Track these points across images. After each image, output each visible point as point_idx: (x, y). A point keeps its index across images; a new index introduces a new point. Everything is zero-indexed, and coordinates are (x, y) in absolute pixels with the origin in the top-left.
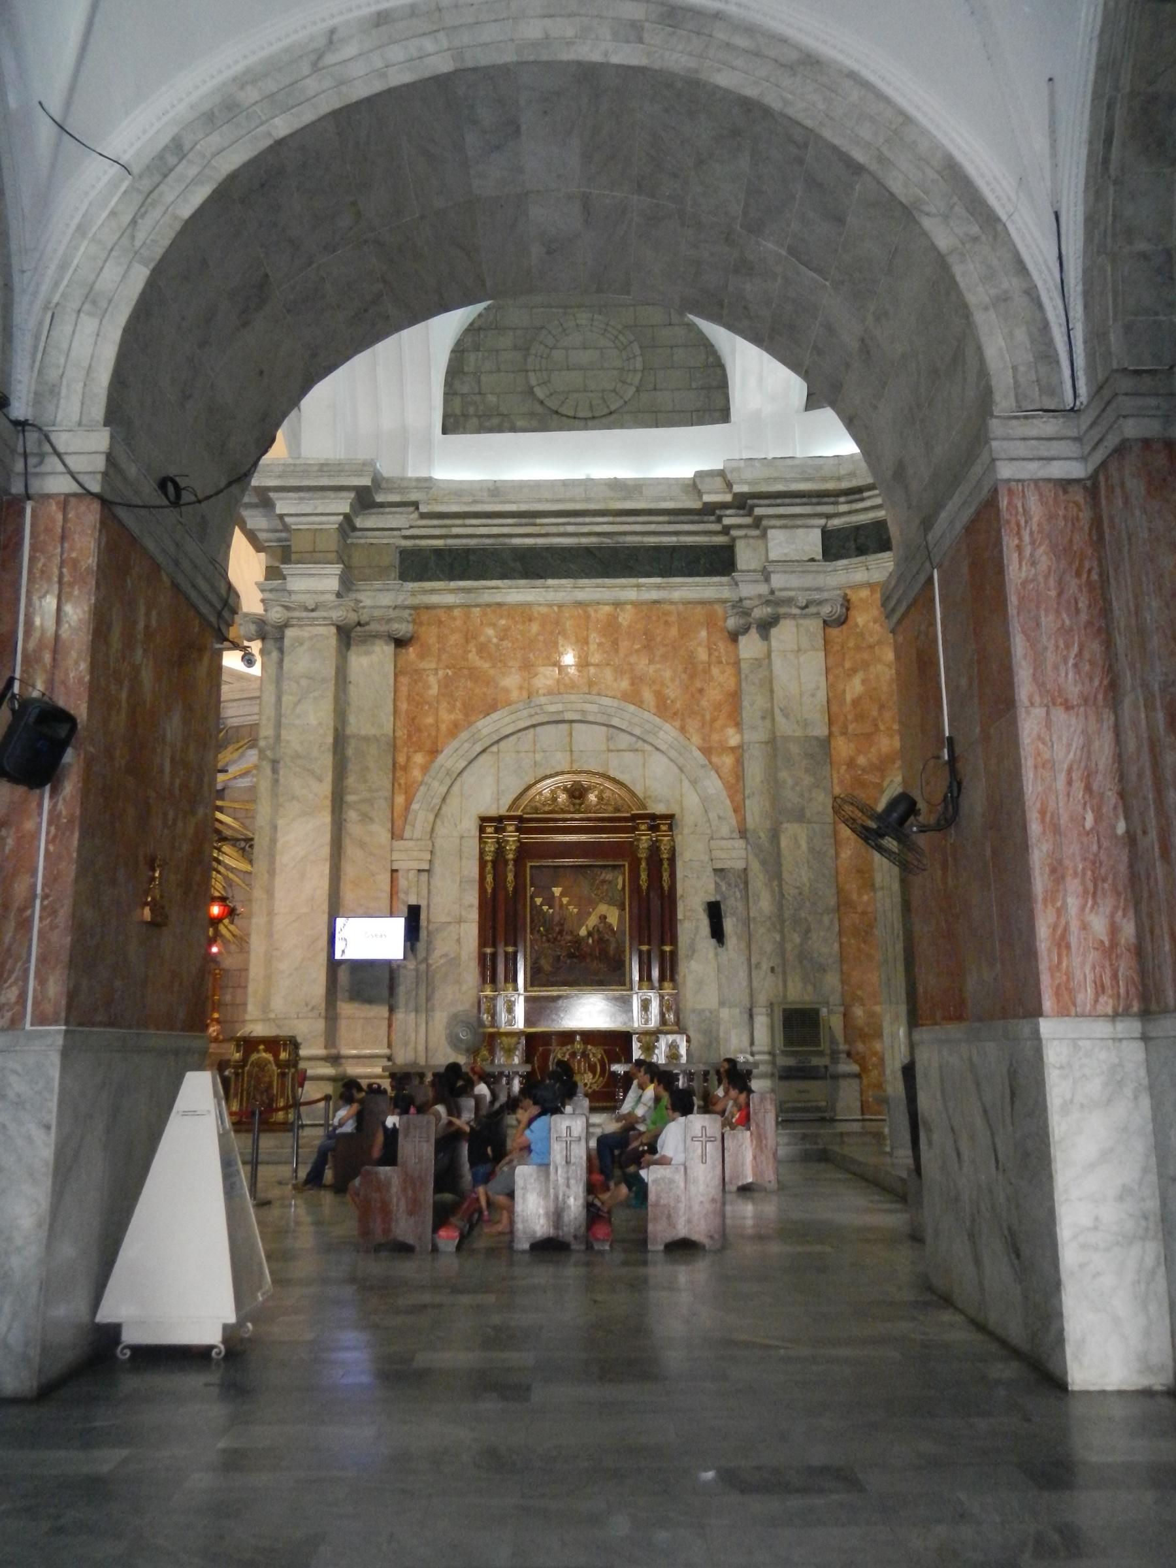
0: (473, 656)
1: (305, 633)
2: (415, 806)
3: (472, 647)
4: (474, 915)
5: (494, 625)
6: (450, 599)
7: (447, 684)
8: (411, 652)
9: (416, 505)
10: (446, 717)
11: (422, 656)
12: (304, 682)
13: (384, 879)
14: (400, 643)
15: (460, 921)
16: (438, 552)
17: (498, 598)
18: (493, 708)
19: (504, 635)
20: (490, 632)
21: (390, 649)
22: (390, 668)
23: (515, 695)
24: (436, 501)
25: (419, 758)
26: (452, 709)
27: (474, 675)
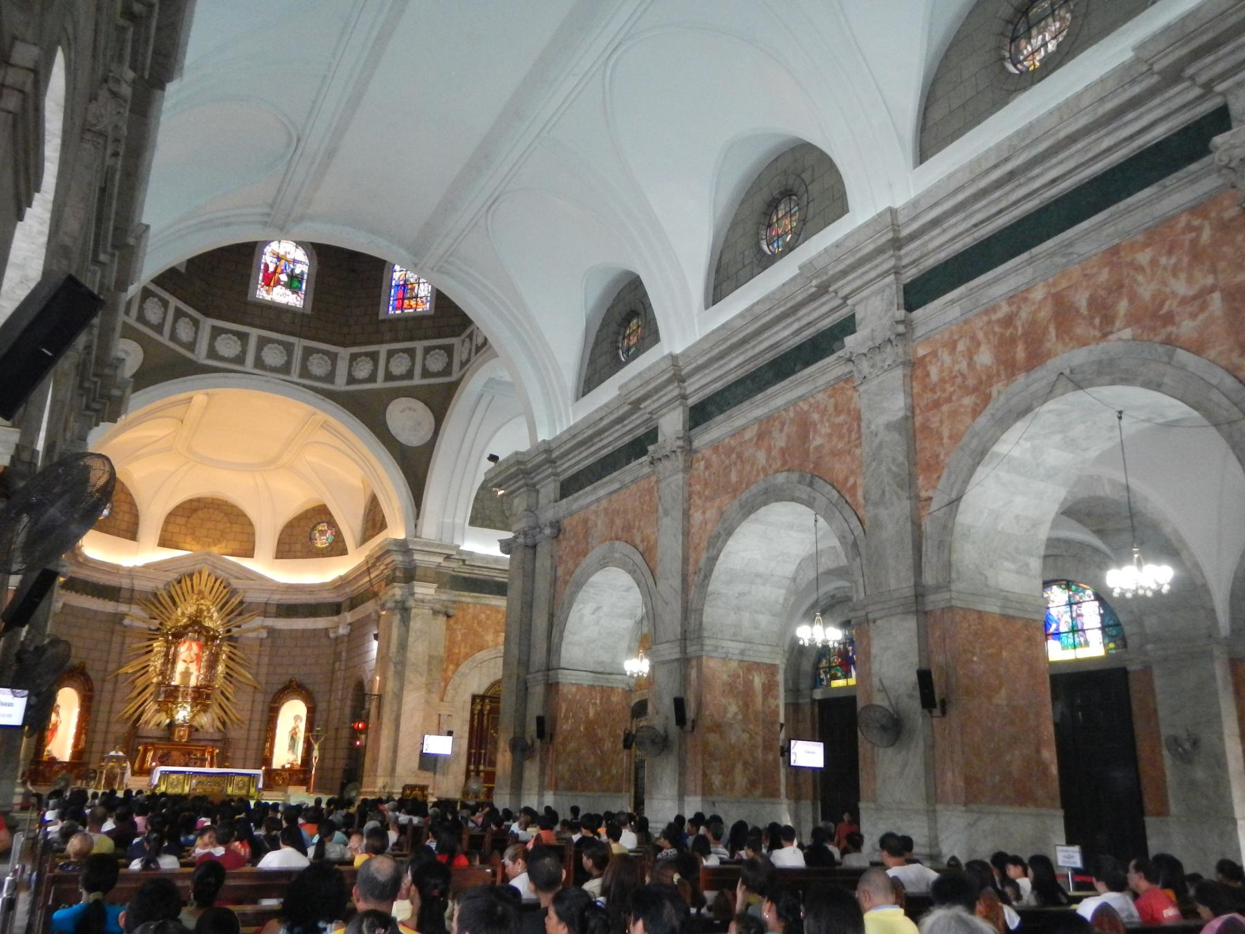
0: (475, 625)
1: (420, 611)
2: (449, 688)
3: (475, 621)
4: (466, 735)
5: (484, 613)
6: (469, 600)
7: (465, 635)
8: (452, 621)
9: (464, 561)
10: (463, 650)
11: (456, 623)
12: (418, 633)
13: (435, 718)
14: (448, 616)
15: (461, 737)
16: (465, 578)
17: (487, 602)
18: (481, 649)
19: (488, 618)
20: (483, 616)
21: (444, 619)
22: (444, 627)
23: (490, 644)
24: (473, 560)
25: (451, 667)
26: (465, 647)
27: (475, 633)
